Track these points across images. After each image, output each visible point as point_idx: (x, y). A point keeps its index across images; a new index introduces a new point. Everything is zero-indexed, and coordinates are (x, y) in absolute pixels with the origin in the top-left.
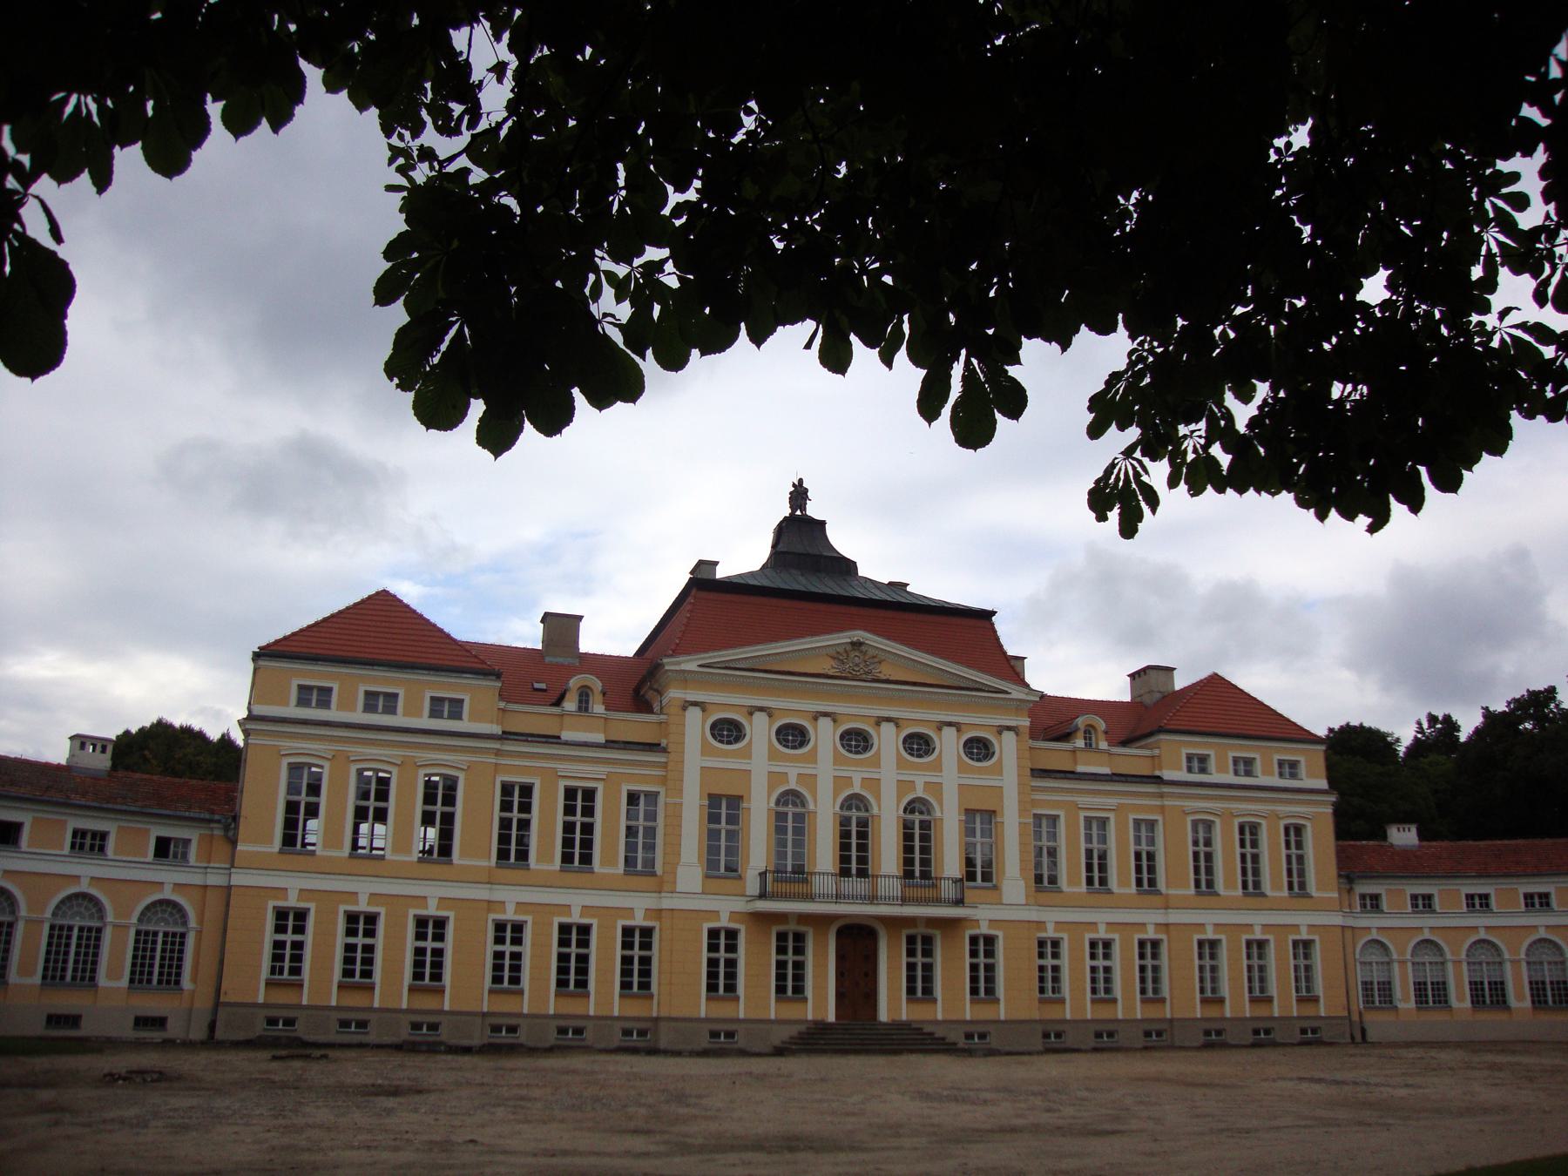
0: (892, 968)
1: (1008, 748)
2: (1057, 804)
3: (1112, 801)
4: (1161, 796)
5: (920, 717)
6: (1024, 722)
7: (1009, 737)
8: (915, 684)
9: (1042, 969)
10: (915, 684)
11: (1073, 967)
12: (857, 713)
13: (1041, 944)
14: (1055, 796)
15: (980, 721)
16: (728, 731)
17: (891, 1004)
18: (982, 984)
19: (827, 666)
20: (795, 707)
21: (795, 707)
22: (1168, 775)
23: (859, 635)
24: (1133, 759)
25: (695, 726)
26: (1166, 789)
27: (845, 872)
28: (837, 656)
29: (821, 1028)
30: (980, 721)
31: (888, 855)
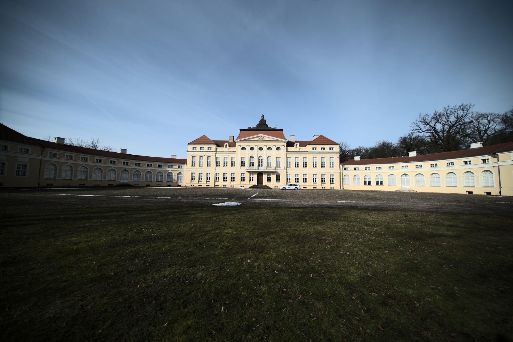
1: (283, 149)
3: (299, 155)
5: (270, 145)
6: (285, 144)
12: (261, 145)
14: (289, 155)
15: (278, 145)
16: (243, 149)
17: (265, 182)
18: (278, 180)
23: (261, 135)
24: (303, 149)
25: (240, 148)
27: (259, 166)
29: (256, 185)
30: (278, 145)
31: (265, 163)
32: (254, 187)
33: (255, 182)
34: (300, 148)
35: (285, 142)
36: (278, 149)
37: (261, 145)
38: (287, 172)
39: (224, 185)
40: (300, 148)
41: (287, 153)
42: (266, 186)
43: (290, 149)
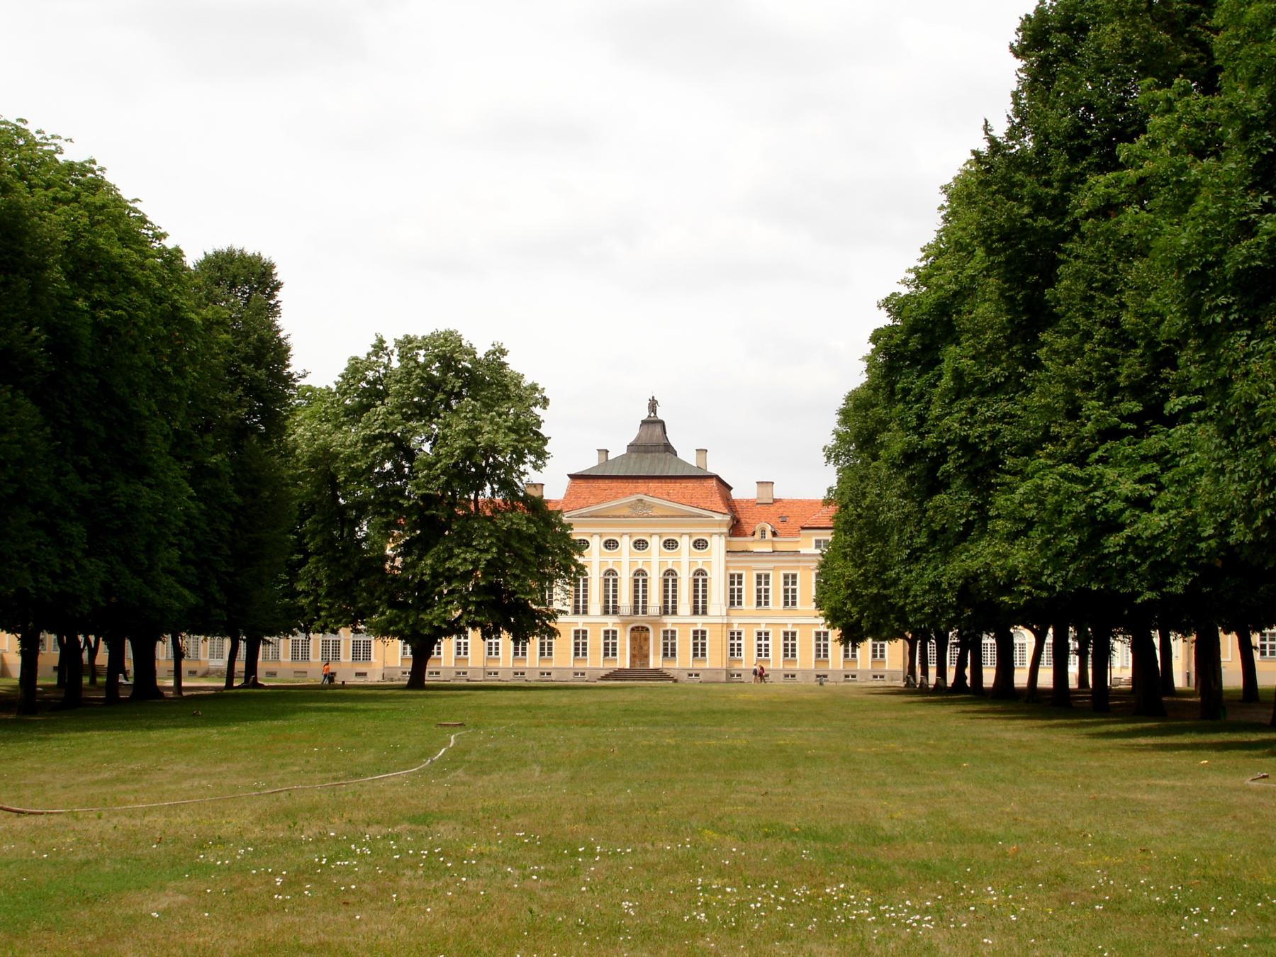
0: (656, 644)
1: (718, 545)
2: (741, 568)
3: (771, 565)
4: (799, 561)
5: (670, 532)
6: (725, 530)
7: (715, 538)
8: (667, 516)
9: (732, 645)
10: (667, 516)
11: (749, 645)
12: (640, 532)
13: (732, 633)
15: (700, 532)
19: (626, 512)
20: (611, 532)
21: (611, 532)
22: (803, 551)
26: (799, 558)
28: (631, 506)
30: (700, 532)
32: (618, 674)
33: (623, 661)
34: (773, 542)
35: (720, 524)
36: (700, 544)
37: (640, 532)
38: (729, 625)
39: (876, 674)
40: (775, 539)
41: (728, 559)
42: (656, 670)
43: (739, 543)
